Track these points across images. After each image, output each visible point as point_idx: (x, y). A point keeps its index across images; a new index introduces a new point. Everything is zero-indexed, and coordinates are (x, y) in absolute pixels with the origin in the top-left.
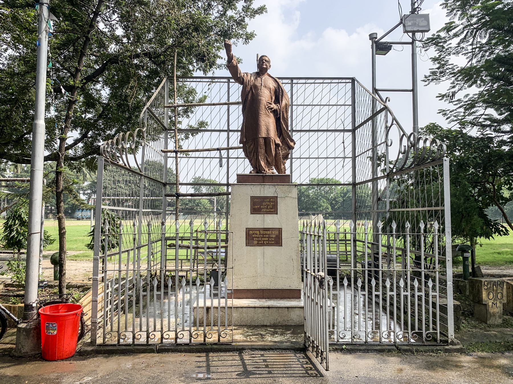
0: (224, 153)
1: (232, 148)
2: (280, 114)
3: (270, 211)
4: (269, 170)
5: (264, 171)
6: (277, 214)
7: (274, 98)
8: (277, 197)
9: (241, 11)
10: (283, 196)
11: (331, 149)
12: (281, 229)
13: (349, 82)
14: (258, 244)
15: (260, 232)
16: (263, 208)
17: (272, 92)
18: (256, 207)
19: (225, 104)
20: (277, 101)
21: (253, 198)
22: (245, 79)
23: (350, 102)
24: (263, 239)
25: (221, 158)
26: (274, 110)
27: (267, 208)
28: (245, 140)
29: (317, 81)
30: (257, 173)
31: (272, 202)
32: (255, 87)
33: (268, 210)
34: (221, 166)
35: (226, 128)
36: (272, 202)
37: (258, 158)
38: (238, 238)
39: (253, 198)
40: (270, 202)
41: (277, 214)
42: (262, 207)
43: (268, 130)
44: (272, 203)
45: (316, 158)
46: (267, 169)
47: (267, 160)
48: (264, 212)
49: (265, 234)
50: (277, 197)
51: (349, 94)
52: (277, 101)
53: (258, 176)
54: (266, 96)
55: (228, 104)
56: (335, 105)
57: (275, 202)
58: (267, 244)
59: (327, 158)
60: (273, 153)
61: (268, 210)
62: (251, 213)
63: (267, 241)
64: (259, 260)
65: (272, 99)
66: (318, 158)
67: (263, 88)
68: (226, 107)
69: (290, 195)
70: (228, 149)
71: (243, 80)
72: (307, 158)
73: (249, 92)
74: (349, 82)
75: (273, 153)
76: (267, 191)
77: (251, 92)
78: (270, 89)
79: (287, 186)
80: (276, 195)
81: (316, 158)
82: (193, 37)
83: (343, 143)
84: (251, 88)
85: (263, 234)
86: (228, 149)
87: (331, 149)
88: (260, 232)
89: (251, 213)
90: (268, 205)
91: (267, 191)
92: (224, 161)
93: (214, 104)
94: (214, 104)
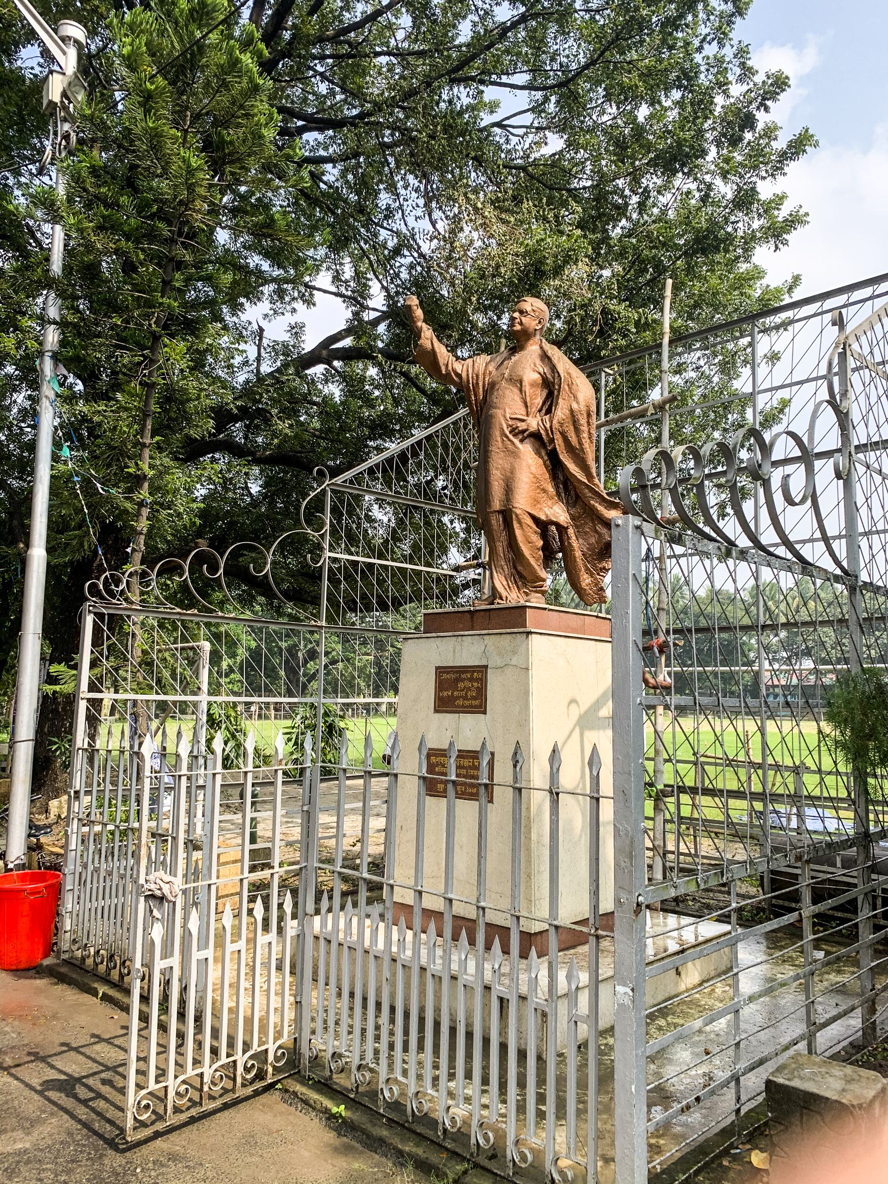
3: (471, 706)
6: (485, 712)
16: (458, 698)
18: (445, 694)
27: (465, 698)
31: (477, 680)
33: (467, 703)
36: (477, 680)
39: (440, 671)
40: (471, 680)
41: (485, 712)
42: (456, 693)
44: (475, 684)
48: (458, 706)
50: (486, 667)
57: (481, 679)
61: (467, 703)
62: (436, 711)
79: (508, 636)
80: (484, 663)
89: (436, 711)
90: (469, 689)
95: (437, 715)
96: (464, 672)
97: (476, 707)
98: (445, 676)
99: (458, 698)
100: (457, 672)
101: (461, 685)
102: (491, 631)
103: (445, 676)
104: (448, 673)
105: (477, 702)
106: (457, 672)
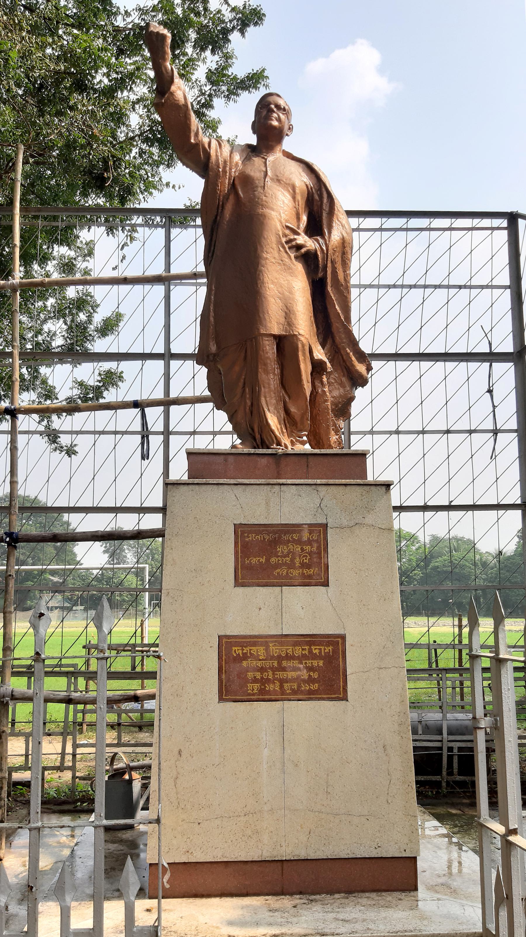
0: (154, 415)
1: (178, 402)
2: (325, 267)
4: (293, 443)
5: (279, 444)
6: (326, 584)
7: (304, 218)
8: (325, 526)
9: (203, 80)
10: (345, 523)
11: (458, 406)
12: (343, 637)
13: (498, 228)
14: (262, 691)
15: (267, 649)
16: (277, 566)
17: (299, 197)
18: (254, 561)
19: (178, 402)
20: (316, 227)
21: (241, 531)
22: (213, 153)
23: (505, 279)
24: (280, 675)
25: (145, 434)
26: (308, 253)
28: (213, 348)
29: (415, 222)
30: (255, 448)
32: (246, 180)
34: (145, 456)
35: (160, 349)
37: (259, 400)
38: (187, 685)
41: (326, 584)
42: (273, 560)
43: (288, 315)
45: (418, 433)
46: (285, 440)
47: (287, 411)
48: (279, 576)
49: (289, 657)
50: (325, 526)
51: (503, 257)
52: (316, 227)
53: (257, 454)
54: (281, 209)
55: (165, 280)
56: (465, 287)
58: (294, 692)
59: (448, 432)
60: (308, 388)
62: (238, 583)
63: (293, 680)
64: (266, 752)
65: (298, 218)
66: (423, 432)
67: (269, 182)
68: (159, 289)
70: (167, 403)
71: (208, 155)
72: (390, 433)
73: (227, 197)
74: (498, 228)
75: (308, 388)
76: (290, 505)
77: (232, 198)
78: (294, 188)
80: (321, 520)
81: (418, 433)
82: (71, 108)
83: (490, 391)
84: (233, 186)
85: (280, 658)
86: (167, 403)
87: (458, 406)
88: (267, 649)
89: (238, 583)
91: (290, 505)
92: (156, 441)
93: (125, 281)
94: (125, 281)
96: (286, 532)
98: (252, 537)
99: (277, 566)
100: (275, 533)
103: (252, 537)
104: (258, 533)
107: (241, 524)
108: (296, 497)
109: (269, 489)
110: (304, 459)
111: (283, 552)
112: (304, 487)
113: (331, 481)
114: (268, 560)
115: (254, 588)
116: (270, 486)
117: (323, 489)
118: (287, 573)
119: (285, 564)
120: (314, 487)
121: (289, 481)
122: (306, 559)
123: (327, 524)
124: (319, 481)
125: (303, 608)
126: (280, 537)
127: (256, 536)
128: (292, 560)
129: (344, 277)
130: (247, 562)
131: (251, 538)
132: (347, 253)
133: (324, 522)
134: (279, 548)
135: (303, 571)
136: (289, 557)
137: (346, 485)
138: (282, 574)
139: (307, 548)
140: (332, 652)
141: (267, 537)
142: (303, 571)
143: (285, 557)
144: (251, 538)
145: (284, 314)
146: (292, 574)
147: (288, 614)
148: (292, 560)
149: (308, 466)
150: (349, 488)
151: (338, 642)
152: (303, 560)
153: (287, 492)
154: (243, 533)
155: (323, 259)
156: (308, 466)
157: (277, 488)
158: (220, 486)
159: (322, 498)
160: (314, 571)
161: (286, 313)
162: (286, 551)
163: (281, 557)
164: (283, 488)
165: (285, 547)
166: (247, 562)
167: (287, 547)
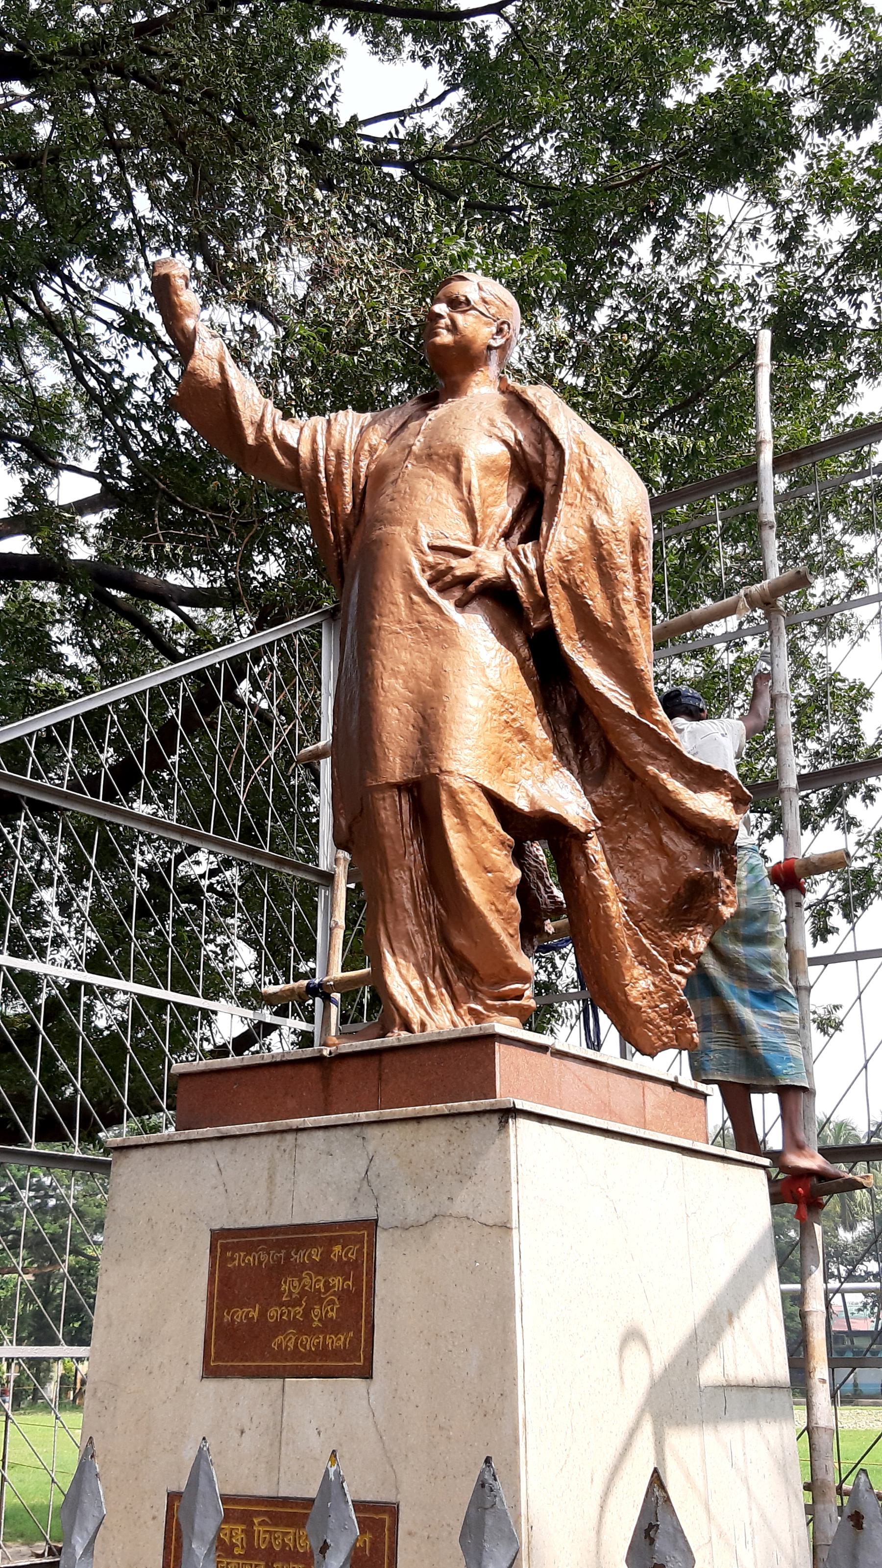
3: (323, 1353)
16: (280, 1327)
27: (304, 1327)
33: (310, 1343)
39: (225, 1242)
40: (324, 1267)
42: (273, 1313)
44: (337, 1282)
48: (282, 1354)
50: (371, 1225)
57: (356, 1265)
61: (310, 1343)
62: (210, 1371)
69: (460, 1207)
79: (441, 1127)
89: (210, 1371)
90: (316, 1298)
95: (212, 1385)
96: (300, 1245)
97: (337, 1354)
98: (240, 1260)
99: (280, 1327)
101: (289, 1286)
102: (388, 1113)
104: (250, 1248)
105: (339, 1341)
106: (278, 1245)
107: (222, 1230)
108: (324, 1156)
109: (276, 1143)
110: (374, 1062)
111: (290, 1294)
112: (340, 1132)
113: (388, 1113)
114: (263, 1314)
115: (235, 1380)
116: (278, 1137)
117: (374, 1133)
118: (296, 1346)
119: (293, 1323)
120: (357, 1130)
121: (310, 1121)
122: (332, 1310)
123: (376, 1221)
124: (363, 1116)
125: (319, 1433)
126: (288, 1257)
127: (245, 1256)
128: (307, 1313)
129: (612, 610)
130: (227, 1318)
131: (236, 1262)
132: (610, 554)
133: (370, 1214)
134: (285, 1282)
135: (325, 1338)
136: (301, 1305)
137: (418, 1119)
138: (287, 1346)
139: (336, 1281)
140: (370, 1549)
141: (264, 1257)
142: (325, 1338)
143: (294, 1307)
144: (236, 1262)
145: (418, 735)
146: (305, 1347)
147: (291, 1446)
148: (307, 1313)
149: (380, 1079)
150: (425, 1125)
151: (383, 1521)
152: (327, 1312)
153: (308, 1148)
154: (225, 1248)
155: (531, 588)
156: (380, 1079)
157: (290, 1137)
158: (194, 1145)
159: (371, 1155)
160: (345, 1339)
161: (421, 731)
162: (296, 1291)
163: (287, 1304)
164: (303, 1137)
165: (296, 1283)
166: (227, 1318)
167: (300, 1282)
